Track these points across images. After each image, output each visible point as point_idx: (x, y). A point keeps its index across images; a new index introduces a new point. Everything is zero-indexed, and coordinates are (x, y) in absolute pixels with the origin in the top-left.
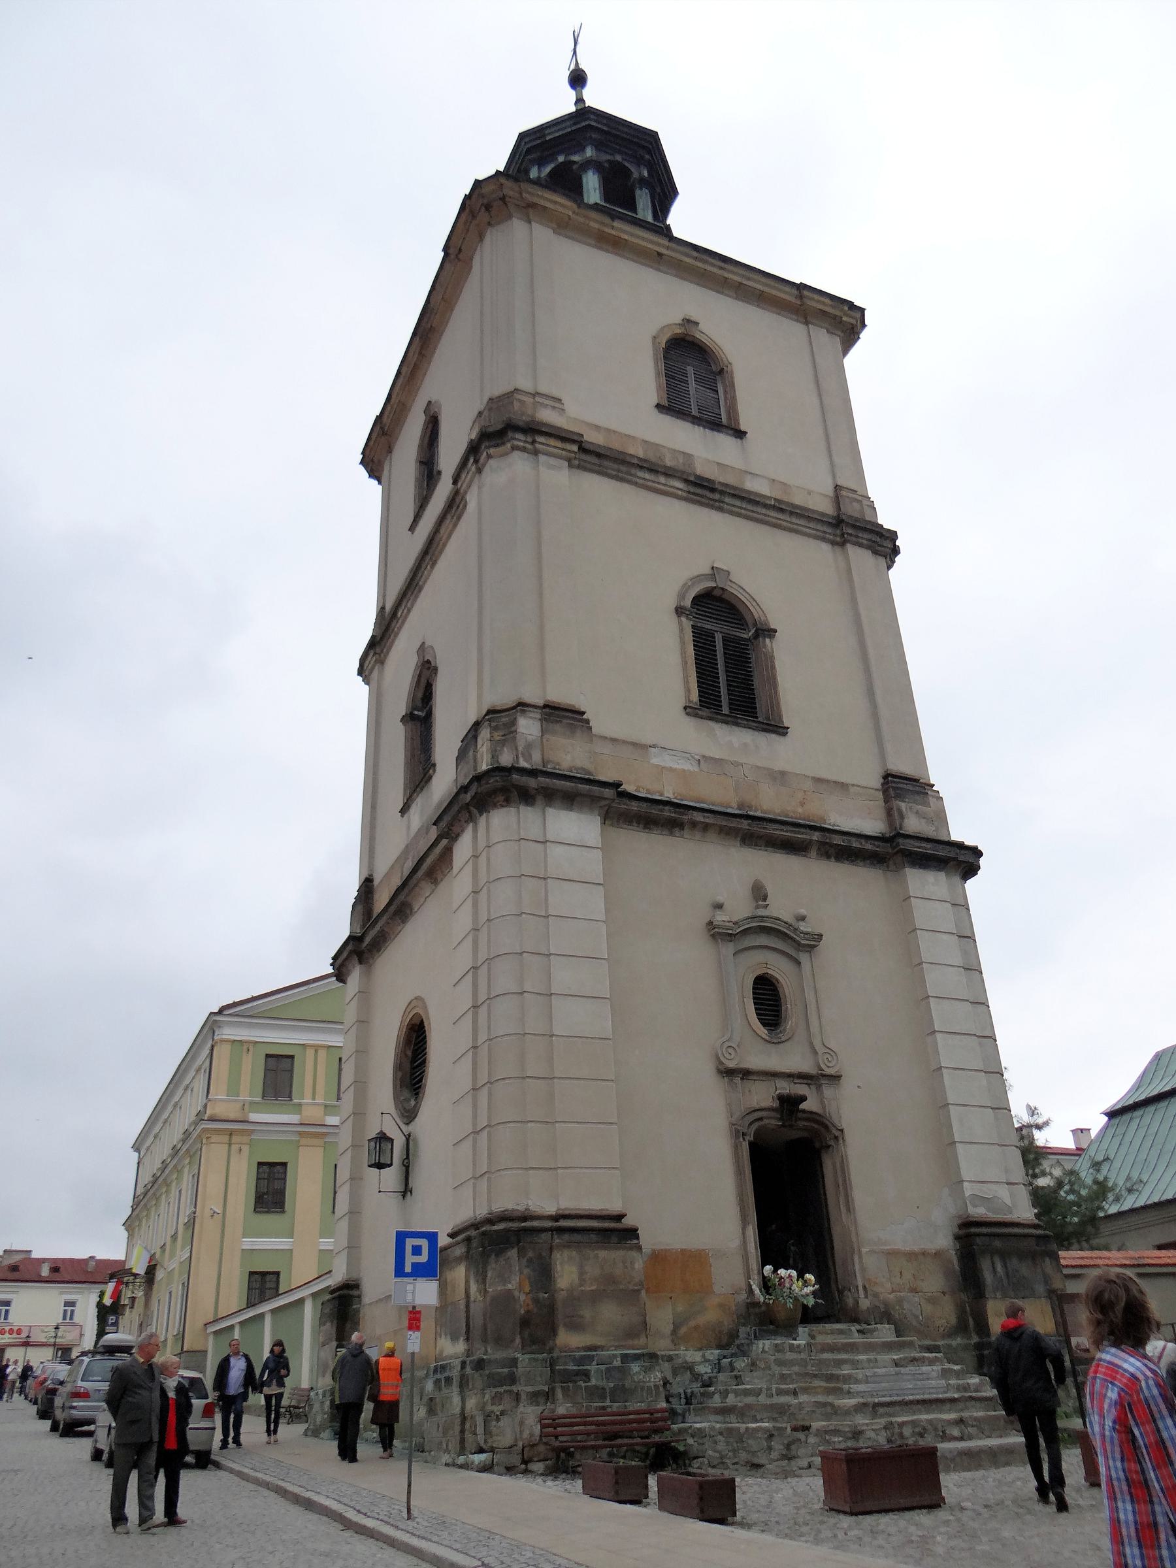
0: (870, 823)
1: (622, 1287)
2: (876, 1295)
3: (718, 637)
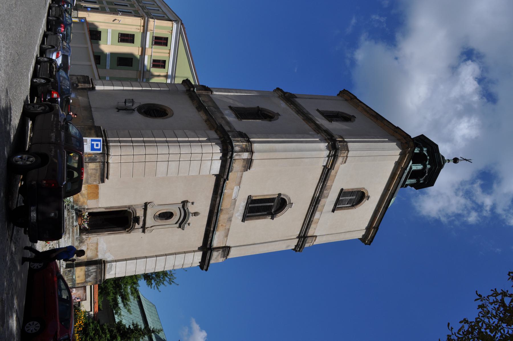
0: (216, 243)
1: (89, 179)
2: (86, 240)
3: (272, 204)
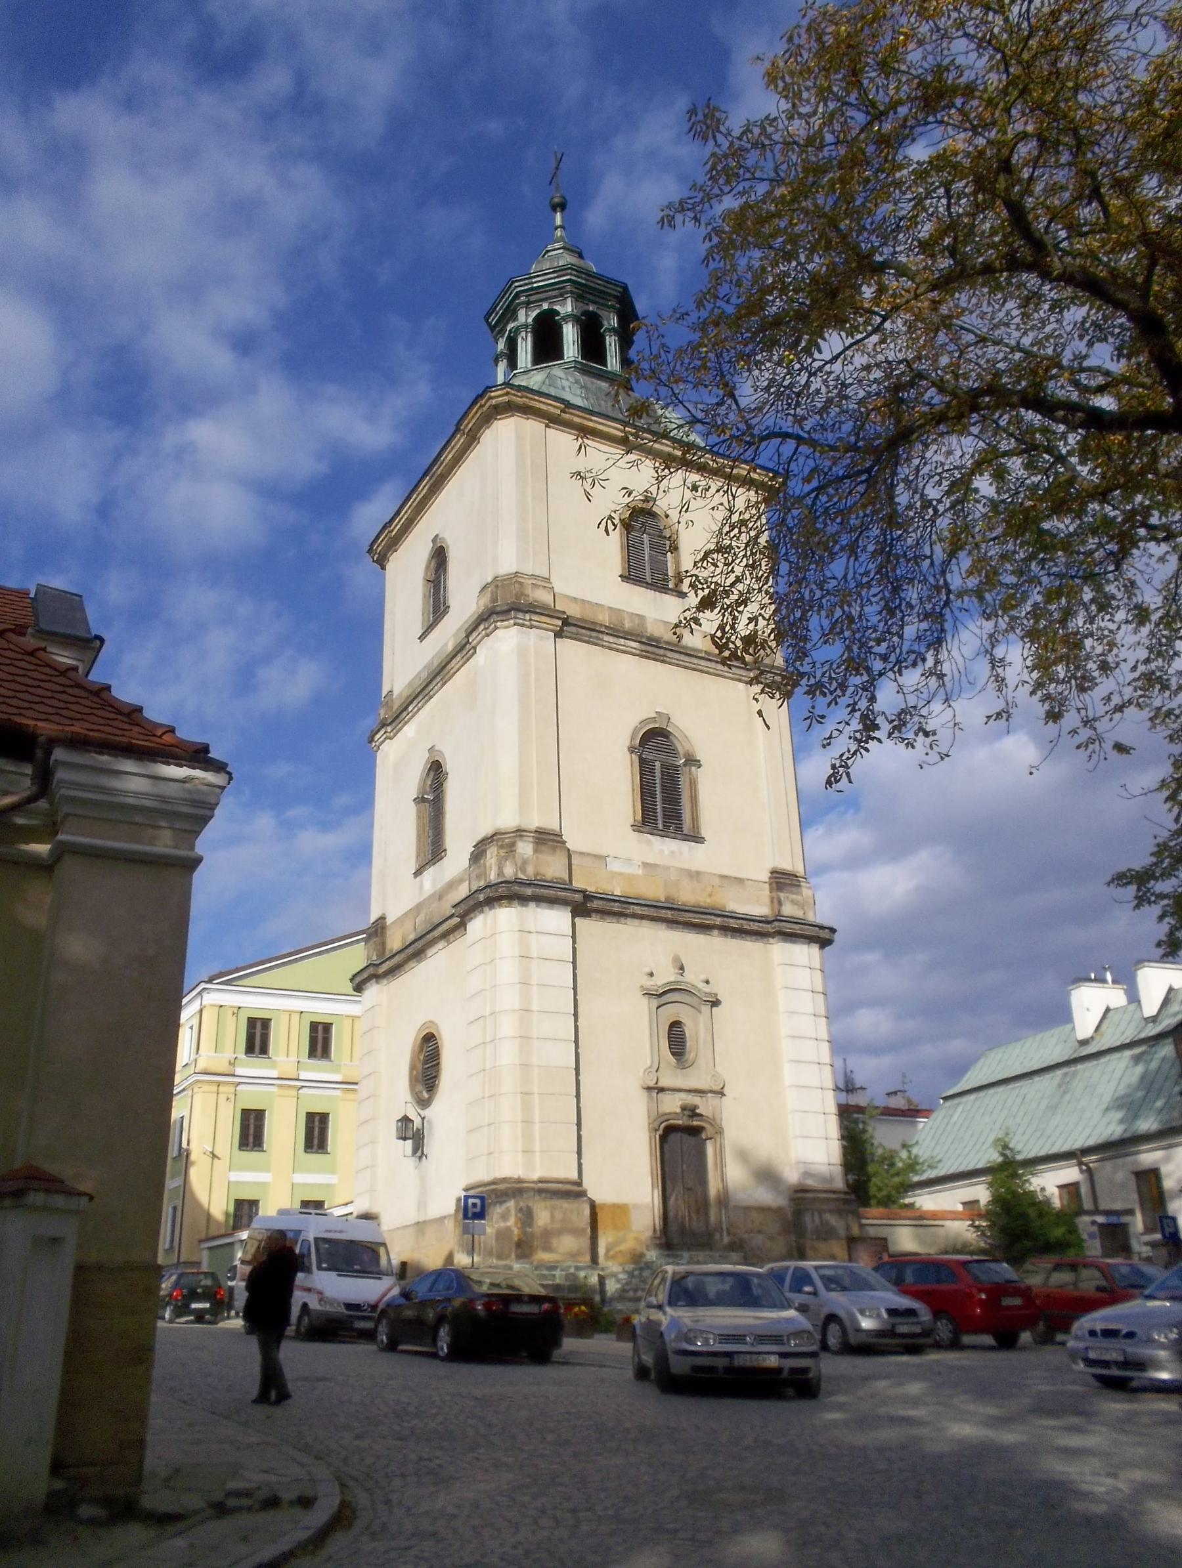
3: (657, 764)
